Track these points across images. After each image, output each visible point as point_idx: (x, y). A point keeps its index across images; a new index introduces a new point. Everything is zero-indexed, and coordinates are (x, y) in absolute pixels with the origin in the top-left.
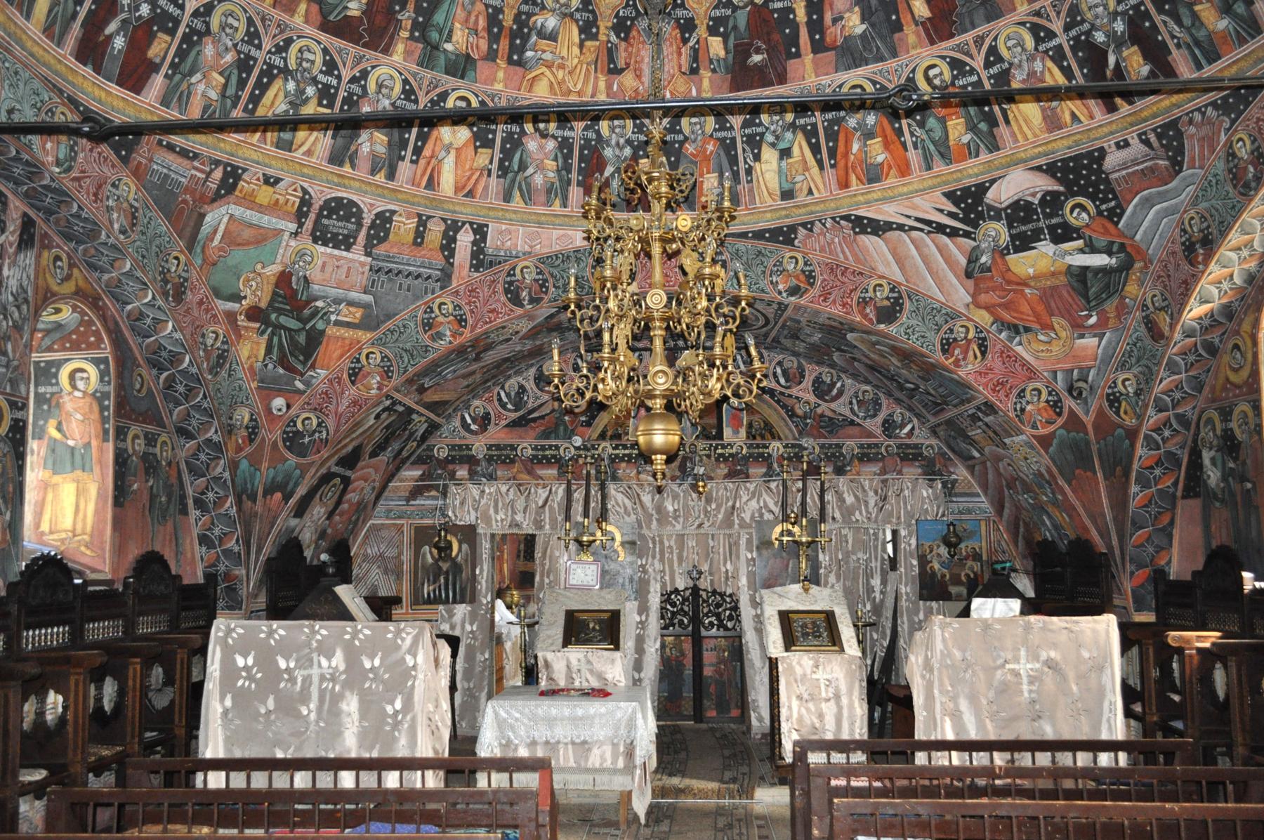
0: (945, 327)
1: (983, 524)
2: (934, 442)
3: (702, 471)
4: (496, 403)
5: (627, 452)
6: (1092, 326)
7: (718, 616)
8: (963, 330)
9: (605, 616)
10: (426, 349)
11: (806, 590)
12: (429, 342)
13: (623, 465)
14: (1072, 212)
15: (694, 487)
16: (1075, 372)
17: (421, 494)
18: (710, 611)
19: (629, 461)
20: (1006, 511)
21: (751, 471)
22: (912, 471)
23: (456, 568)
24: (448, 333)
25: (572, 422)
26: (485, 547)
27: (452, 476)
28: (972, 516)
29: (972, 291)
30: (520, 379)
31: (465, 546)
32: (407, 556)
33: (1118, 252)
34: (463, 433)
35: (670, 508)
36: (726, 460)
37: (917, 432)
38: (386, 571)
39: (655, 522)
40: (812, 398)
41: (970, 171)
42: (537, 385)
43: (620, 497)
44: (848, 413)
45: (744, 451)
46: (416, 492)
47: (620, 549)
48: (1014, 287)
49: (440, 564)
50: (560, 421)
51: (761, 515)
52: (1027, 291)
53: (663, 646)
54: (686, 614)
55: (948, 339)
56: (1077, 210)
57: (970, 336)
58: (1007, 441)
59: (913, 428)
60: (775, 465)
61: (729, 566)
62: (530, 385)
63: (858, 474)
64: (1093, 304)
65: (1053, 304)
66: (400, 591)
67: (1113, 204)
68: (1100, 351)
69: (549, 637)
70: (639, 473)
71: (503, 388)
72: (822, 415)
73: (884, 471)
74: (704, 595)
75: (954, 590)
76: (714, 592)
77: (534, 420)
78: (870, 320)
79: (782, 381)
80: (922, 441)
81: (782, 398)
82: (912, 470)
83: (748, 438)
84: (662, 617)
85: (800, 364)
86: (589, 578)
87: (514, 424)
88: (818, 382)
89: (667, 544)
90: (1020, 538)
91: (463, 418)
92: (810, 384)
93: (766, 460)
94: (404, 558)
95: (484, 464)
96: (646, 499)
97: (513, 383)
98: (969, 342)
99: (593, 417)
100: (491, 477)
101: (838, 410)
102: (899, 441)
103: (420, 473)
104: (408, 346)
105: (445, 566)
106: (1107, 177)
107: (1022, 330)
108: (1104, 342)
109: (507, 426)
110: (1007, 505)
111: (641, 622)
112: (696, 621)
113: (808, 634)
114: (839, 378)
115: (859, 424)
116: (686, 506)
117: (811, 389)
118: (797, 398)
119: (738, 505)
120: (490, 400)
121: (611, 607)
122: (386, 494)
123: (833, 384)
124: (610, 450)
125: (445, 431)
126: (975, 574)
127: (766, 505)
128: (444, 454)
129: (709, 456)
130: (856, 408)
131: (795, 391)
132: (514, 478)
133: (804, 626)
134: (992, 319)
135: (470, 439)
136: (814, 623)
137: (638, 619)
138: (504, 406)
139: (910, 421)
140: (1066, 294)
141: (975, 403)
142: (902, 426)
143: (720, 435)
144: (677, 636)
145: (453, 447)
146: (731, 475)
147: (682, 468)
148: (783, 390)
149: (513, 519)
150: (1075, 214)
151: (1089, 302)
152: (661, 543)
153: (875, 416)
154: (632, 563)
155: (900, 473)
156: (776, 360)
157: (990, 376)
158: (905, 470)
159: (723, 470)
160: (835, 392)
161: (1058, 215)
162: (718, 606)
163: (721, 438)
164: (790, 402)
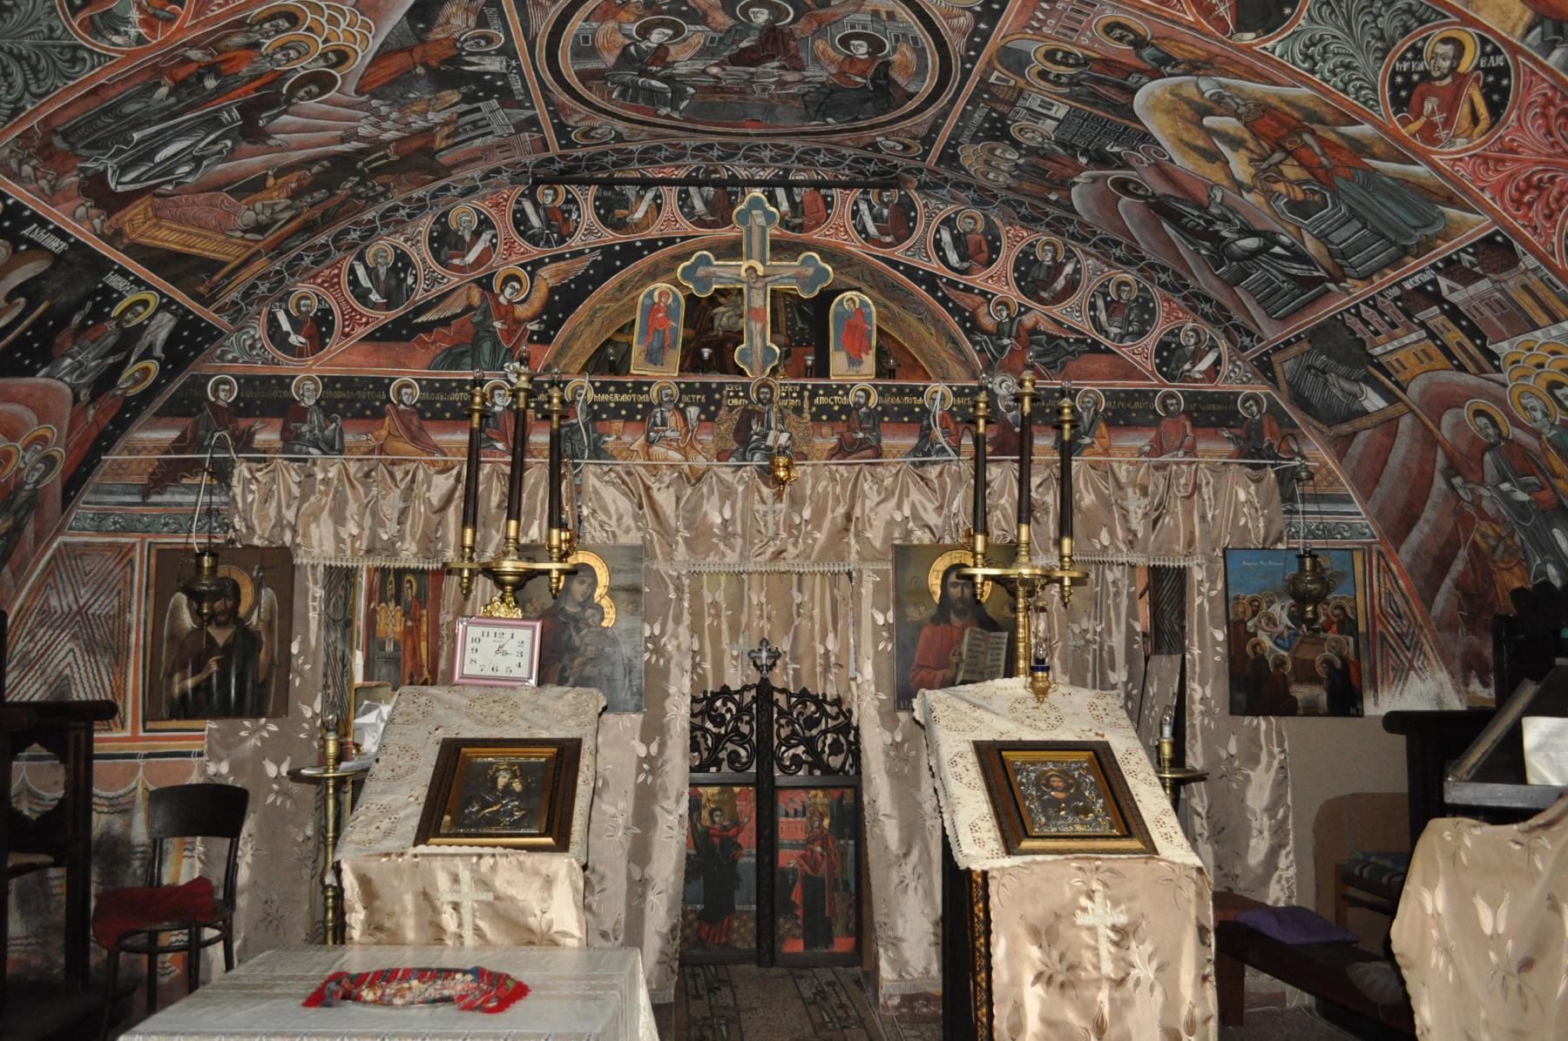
0: (1403, 44)
1: (1358, 557)
2: (1261, 389)
3: (784, 439)
4: (346, 289)
5: (625, 398)
7: (810, 744)
8: (1448, 49)
9: (541, 756)
10: (74, 55)
11: (1041, 693)
12: (82, 39)
13: (618, 424)
15: (768, 474)
17: (176, 480)
18: (794, 732)
19: (629, 418)
20: (1415, 536)
21: (886, 442)
22: (1216, 448)
23: (247, 641)
24: (135, 15)
25: (510, 333)
26: (313, 596)
27: (244, 442)
28: (1337, 543)
30: (399, 240)
31: (267, 594)
32: (138, 615)
34: (273, 352)
35: (717, 519)
36: (834, 417)
37: (1226, 368)
38: (91, 647)
39: (682, 548)
40: (1015, 296)
42: (436, 254)
43: (611, 495)
44: (1086, 327)
45: (874, 400)
46: (166, 475)
47: (606, 602)
49: (212, 631)
50: (482, 332)
51: (909, 533)
53: (695, 806)
54: (743, 739)
55: (1407, 75)
57: (1466, 65)
58: (1503, 348)
59: (1218, 362)
60: (937, 431)
61: (831, 644)
62: (421, 254)
63: (1106, 452)
66: (120, 689)
69: (386, 811)
70: (650, 443)
71: (361, 258)
72: (1034, 331)
73: (1158, 449)
74: (781, 699)
75: (1301, 692)
76: (804, 696)
77: (428, 327)
78: (1220, 22)
79: (953, 258)
80: (1236, 388)
81: (952, 293)
82: (1215, 446)
83: (879, 375)
84: (695, 746)
85: (990, 227)
86: (511, 661)
87: (385, 335)
88: (1026, 262)
89: (708, 598)
90: (1448, 582)
91: (273, 321)
92: (1010, 266)
93: (918, 419)
94: (132, 618)
95: (316, 418)
96: (665, 499)
97: (382, 248)
98: (1460, 80)
99: (556, 325)
100: (330, 446)
101: (1069, 321)
102: (1189, 387)
103: (173, 434)
104: (25, 46)
105: (221, 636)
109: (370, 338)
110: (1429, 513)
111: (648, 758)
112: (764, 753)
113: (1055, 804)
114: (1070, 255)
115: (1108, 351)
116: (748, 513)
117: (1012, 276)
118: (983, 293)
119: (857, 512)
120: (332, 283)
121: (558, 733)
122: (96, 479)
123: (1057, 268)
124: (591, 396)
125: (233, 346)
126: (1344, 660)
127: (916, 516)
128: (226, 397)
129: (798, 410)
130: (1103, 317)
131: (978, 280)
132: (382, 450)
133: (1043, 782)
134: (1528, 15)
135: (287, 366)
136: (1065, 774)
137: (642, 751)
138: (362, 296)
139: (1213, 346)
141: (1444, 249)
142: (1197, 357)
143: (822, 368)
144: (725, 785)
145: (247, 382)
146: (844, 450)
147: (742, 433)
148: (954, 276)
149: (374, 535)
152: (696, 595)
153: (1141, 334)
154: (632, 633)
155: (1191, 451)
156: (942, 215)
157: (1510, 167)
158: (1201, 446)
159: (827, 440)
160: (1060, 283)
162: (811, 723)
163: (826, 375)
164: (967, 301)
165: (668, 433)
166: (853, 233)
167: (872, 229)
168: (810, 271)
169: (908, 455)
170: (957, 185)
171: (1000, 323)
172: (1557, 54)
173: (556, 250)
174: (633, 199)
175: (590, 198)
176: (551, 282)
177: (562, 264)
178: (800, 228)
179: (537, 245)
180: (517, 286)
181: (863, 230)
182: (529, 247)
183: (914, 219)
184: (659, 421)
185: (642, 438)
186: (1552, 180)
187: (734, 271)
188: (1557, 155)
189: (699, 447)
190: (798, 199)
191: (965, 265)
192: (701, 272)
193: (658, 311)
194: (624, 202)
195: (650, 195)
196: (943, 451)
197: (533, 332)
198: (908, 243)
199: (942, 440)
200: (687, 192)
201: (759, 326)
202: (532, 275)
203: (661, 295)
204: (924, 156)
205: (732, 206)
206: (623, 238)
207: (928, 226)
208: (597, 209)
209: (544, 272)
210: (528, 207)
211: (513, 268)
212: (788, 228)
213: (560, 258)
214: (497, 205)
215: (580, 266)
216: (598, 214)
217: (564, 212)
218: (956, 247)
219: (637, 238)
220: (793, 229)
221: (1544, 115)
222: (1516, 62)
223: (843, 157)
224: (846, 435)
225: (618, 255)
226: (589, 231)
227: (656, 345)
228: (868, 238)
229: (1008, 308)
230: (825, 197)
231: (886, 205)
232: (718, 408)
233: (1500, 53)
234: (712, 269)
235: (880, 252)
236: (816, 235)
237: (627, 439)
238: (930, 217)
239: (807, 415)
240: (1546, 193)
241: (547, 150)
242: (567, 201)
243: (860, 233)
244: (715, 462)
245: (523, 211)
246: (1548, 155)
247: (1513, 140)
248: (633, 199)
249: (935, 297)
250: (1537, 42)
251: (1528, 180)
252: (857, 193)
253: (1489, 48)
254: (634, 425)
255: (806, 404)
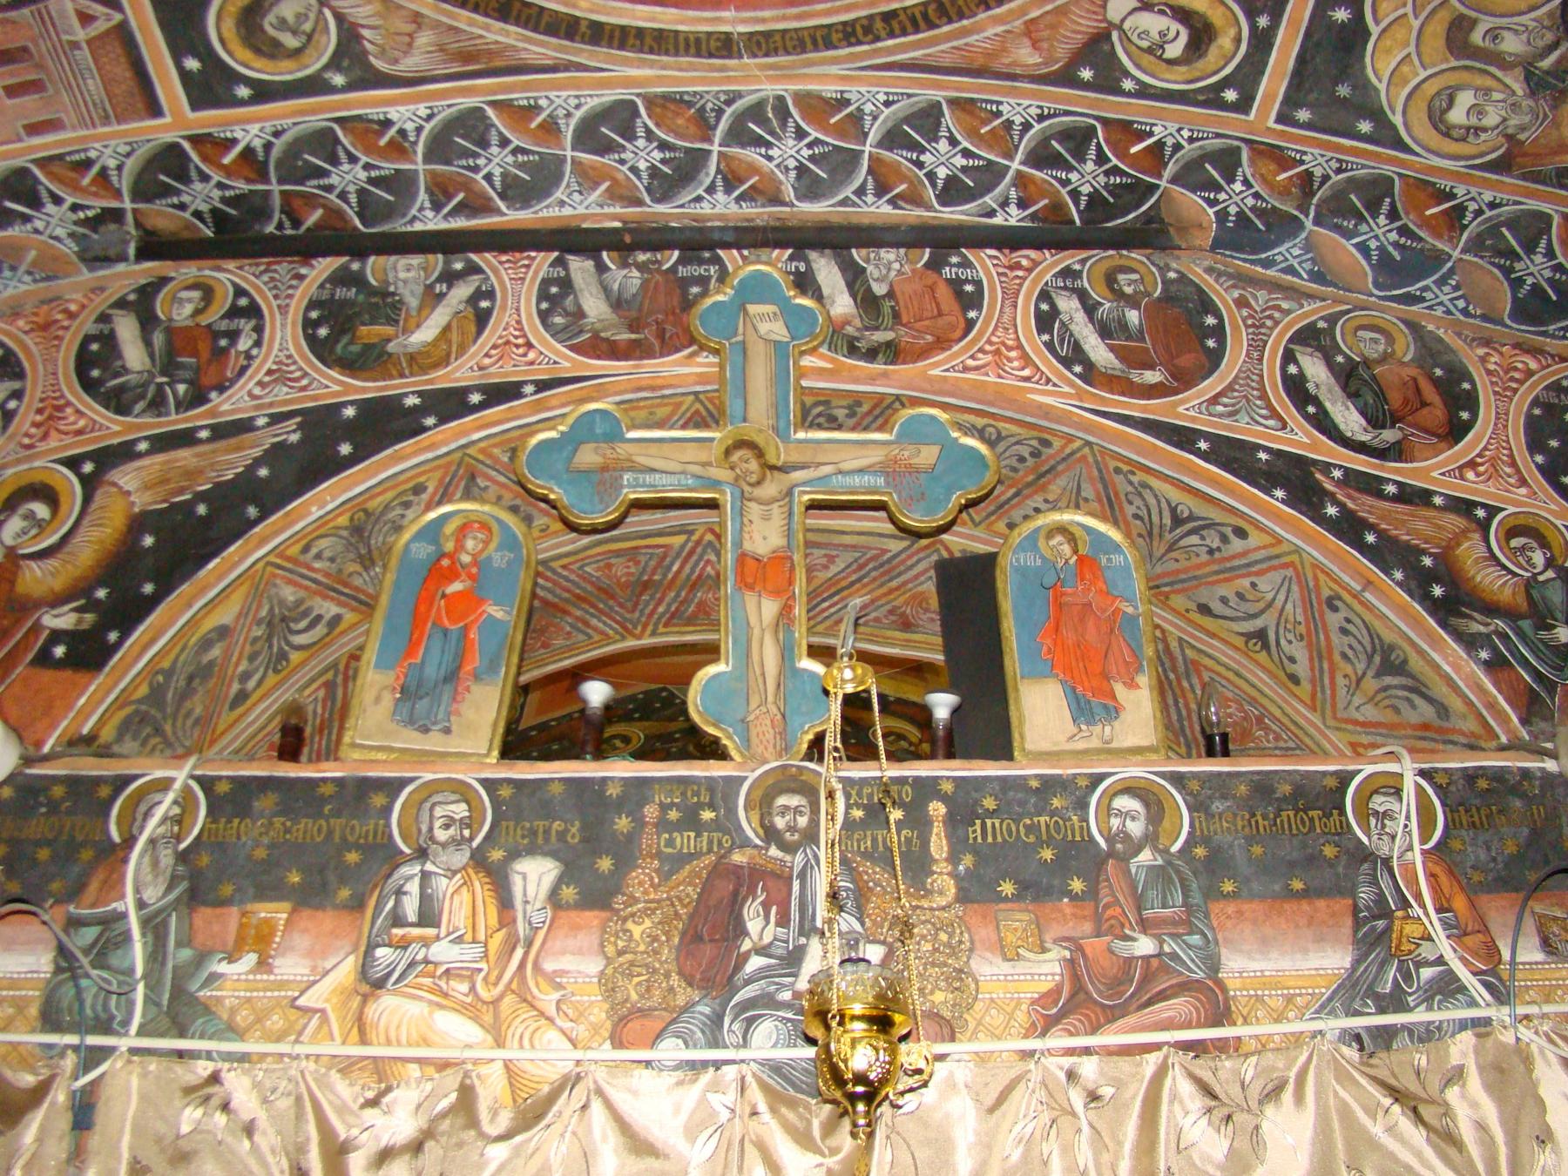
19: (311, 896)
70: (373, 983)
79: (1350, 420)
81: (1363, 506)
92: (1517, 437)
117: (1529, 464)
118: (1463, 507)
148: (1362, 464)
163: (1000, 745)
164: (1413, 527)
165: (444, 952)
166: (1048, 364)
167: (1099, 352)
168: (928, 455)
169: (1326, 1009)
170: (1337, 211)
171: (1530, 584)
173: (175, 421)
174: (413, 302)
175: (297, 305)
176: (142, 501)
177: (184, 456)
178: (893, 352)
179: (123, 410)
180: (41, 510)
181: (1075, 356)
182: (97, 412)
183: (1219, 332)
184: (411, 907)
185: (346, 969)
187: (692, 453)
189: (548, 999)
190: (879, 289)
191: (1389, 435)
192: (588, 456)
193: (452, 574)
194: (385, 305)
195: (462, 291)
196: (1448, 988)
197: (56, 636)
198: (1211, 386)
199: (1444, 945)
200: (566, 284)
201: (770, 608)
202: (90, 485)
203: (464, 529)
204: (1247, 77)
205: (688, 305)
206: (369, 388)
207: (1258, 346)
208: (309, 325)
209: (127, 477)
210: (127, 329)
211: (45, 466)
212: (853, 350)
213: (185, 438)
214: (45, 327)
215: (232, 461)
216: (312, 341)
217: (216, 335)
218: (1353, 395)
219: (408, 389)
220: (871, 354)
223: (1004, 138)
224: (1094, 946)
225: (350, 430)
226: (279, 375)
227: (431, 672)
228: (1090, 373)
229: (1544, 544)
230: (956, 284)
231: (1132, 301)
232: (625, 861)
234: (622, 450)
235: (1136, 407)
236: (937, 367)
237: (290, 966)
238: (1259, 331)
239: (944, 883)
241: (155, 110)
242: (234, 312)
243: (1067, 362)
244: (607, 1052)
245: (109, 341)
248: (413, 302)
249: (1320, 519)
252: (1051, 263)
254: (327, 920)
255: (939, 845)
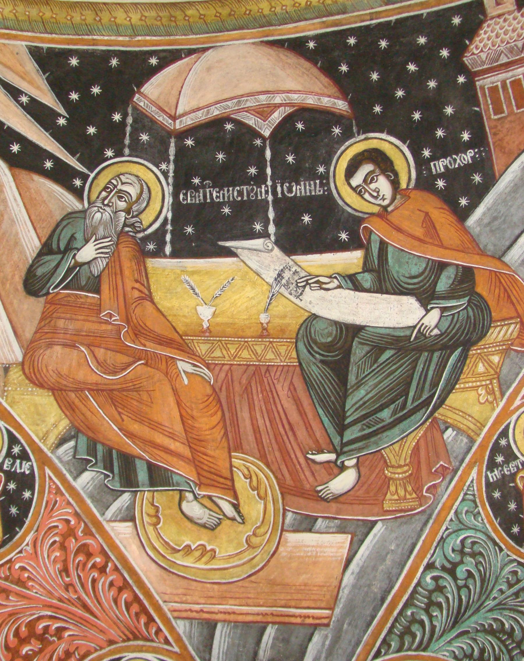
6: (337, 498)
14: (350, 172)
16: (270, 632)
29: (28, 333)
33: (450, 295)
41: (120, 16)
48: (151, 347)
52: (183, 366)
56: (367, 168)
64: (350, 434)
65: (244, 415)
67: (468, 157)
68: (349, 579)
106: (470, 84)
107: (142, 475)
108: (364, 551)
134: (64, 424)
140: (283, 390)
150: (357, 180)
151: (341, 429)
161: (313, 175)
172: (87, 476)
186: (60, 630)
188: (69, 601)
221: (63, 547)
222: (43, 475)
233: (28, 459)
240: (50, 648)
246: (60, 600)
247: (23, 569)
250: (68, 458)
251: (31, 625)
253: (16, 450)
